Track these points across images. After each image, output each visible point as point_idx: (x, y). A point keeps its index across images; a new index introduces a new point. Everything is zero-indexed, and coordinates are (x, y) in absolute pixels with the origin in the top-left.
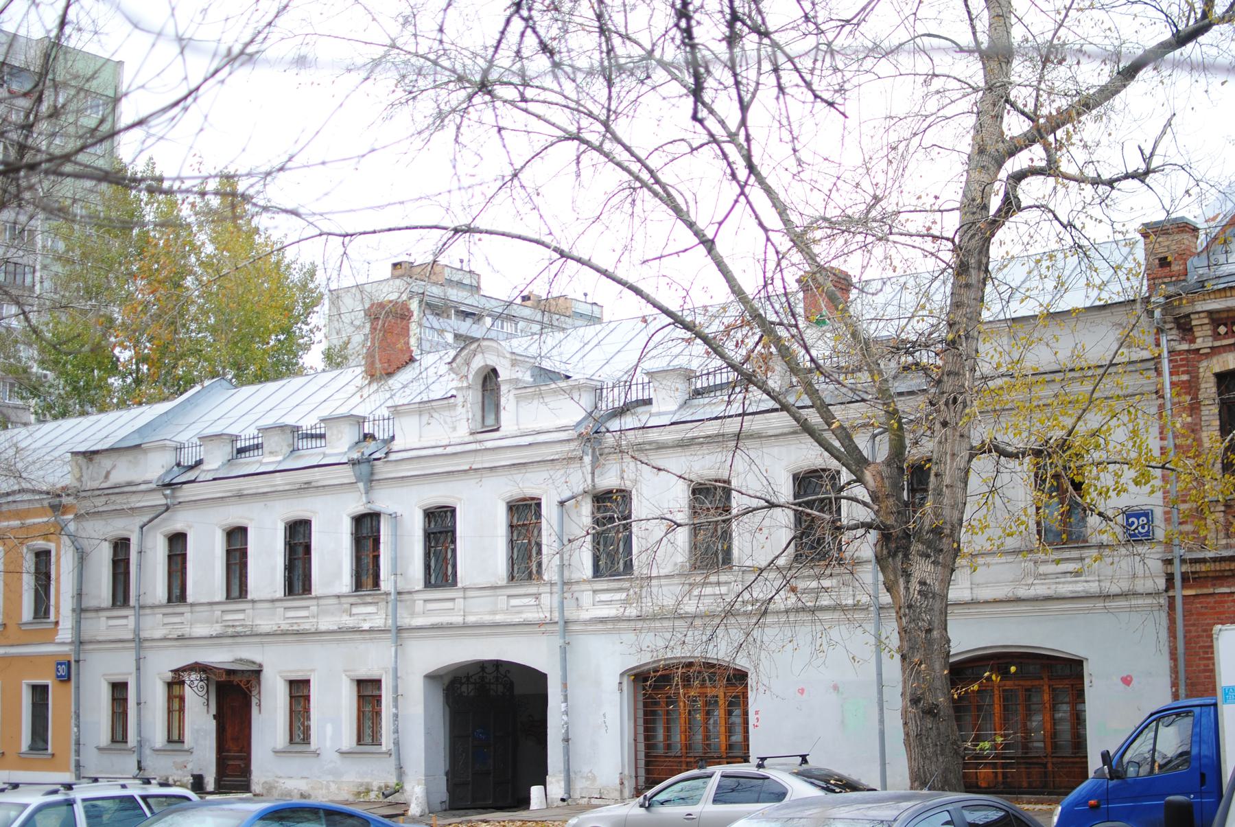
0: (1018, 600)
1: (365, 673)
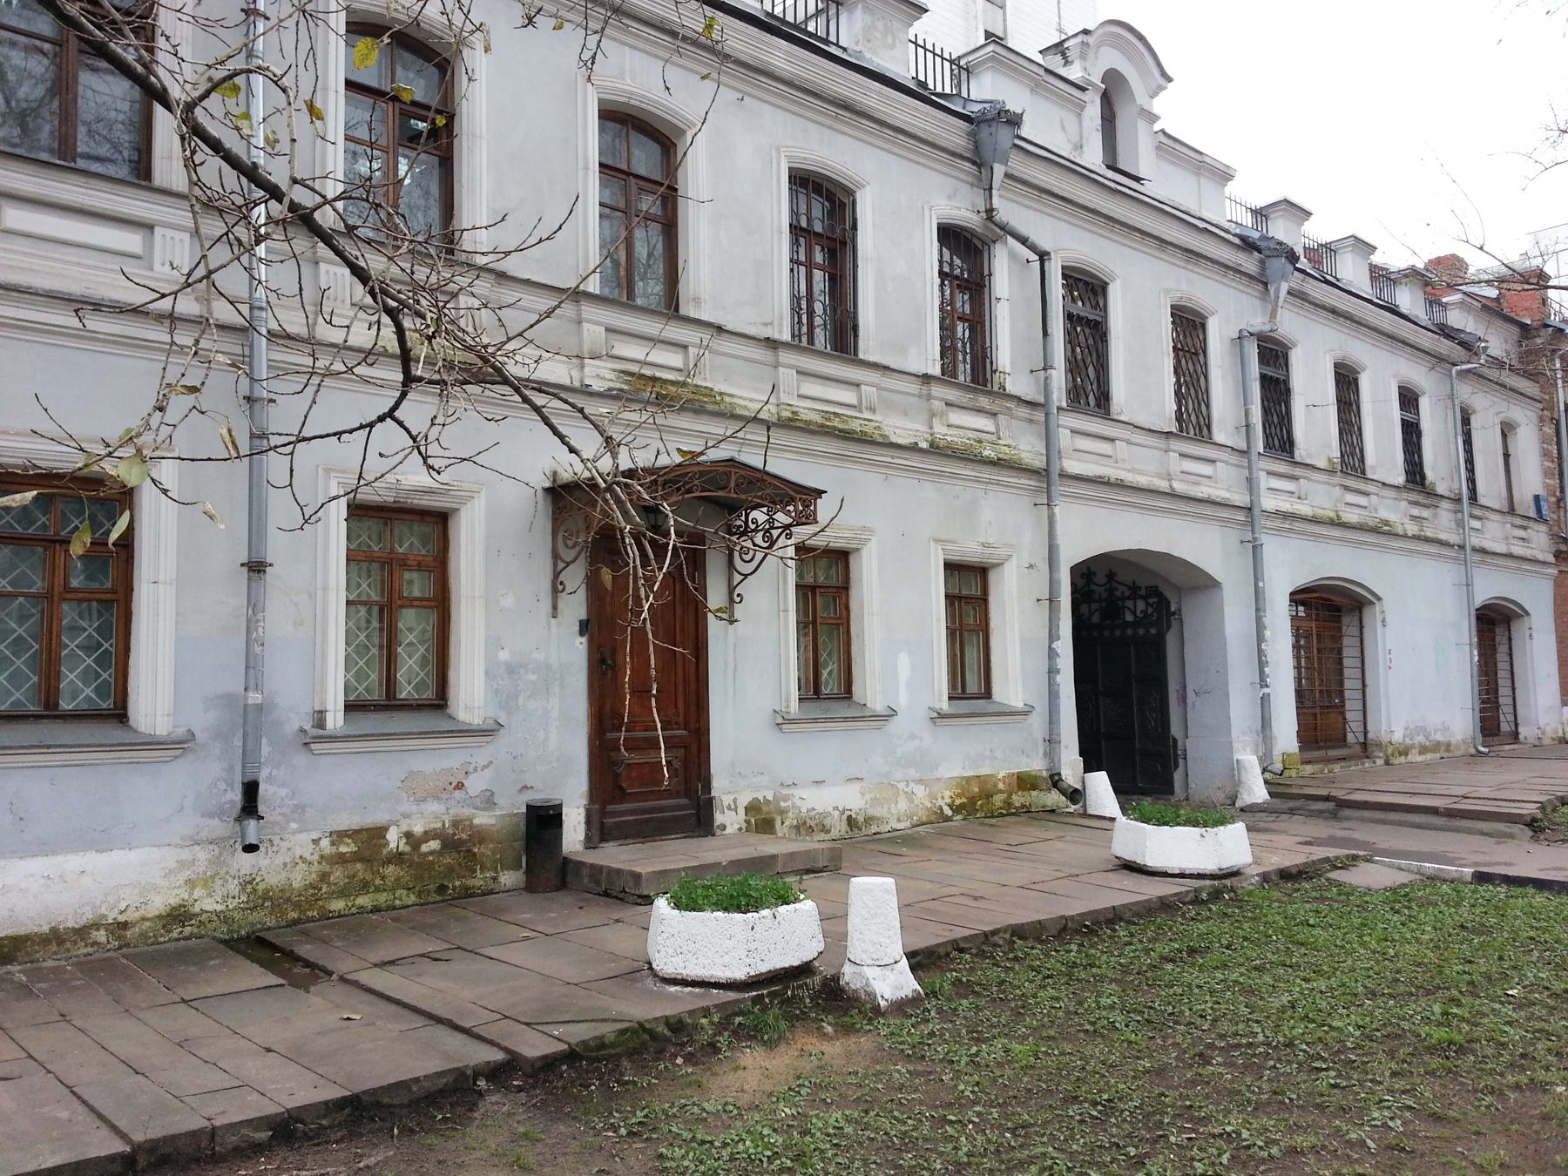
0: (1510, 556)
1: (970, 550)
